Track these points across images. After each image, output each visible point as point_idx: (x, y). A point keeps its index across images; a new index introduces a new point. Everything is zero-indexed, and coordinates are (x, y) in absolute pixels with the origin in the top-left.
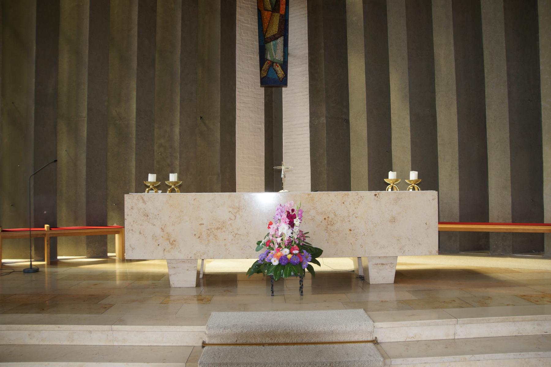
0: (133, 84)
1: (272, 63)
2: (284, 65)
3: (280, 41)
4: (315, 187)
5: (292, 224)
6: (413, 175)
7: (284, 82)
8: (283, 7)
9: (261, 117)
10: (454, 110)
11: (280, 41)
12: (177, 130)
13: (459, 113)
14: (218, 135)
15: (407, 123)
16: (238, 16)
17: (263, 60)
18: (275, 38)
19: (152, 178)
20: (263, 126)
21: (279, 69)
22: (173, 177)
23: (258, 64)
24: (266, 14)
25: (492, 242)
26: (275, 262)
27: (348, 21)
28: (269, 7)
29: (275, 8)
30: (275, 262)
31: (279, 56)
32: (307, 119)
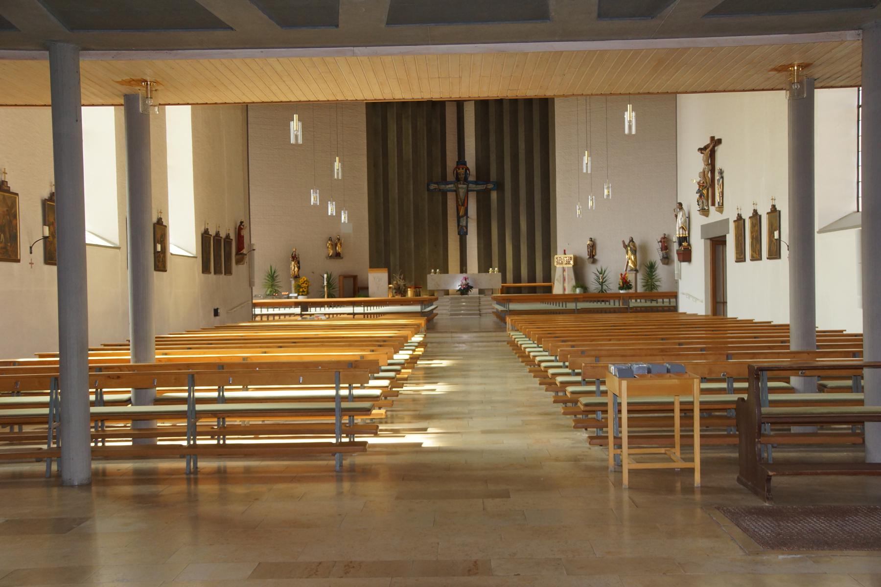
0: (412, 236)
1: (462, 226)
2: (467, 227)
3: (465, 218)
4: (480, 271)
5: (466, 280)
6: (496, 269)
7: (466, 233)
8: (466, 204)
9: (458, 243)
10: (526, 244)
11: (465, 218)
12: (427, 252)
13: (527, 245)
14: (441, 252)
15: (511, 248)
16: (448, 203)
17: (459, 225)
18: (463, 217)
19: (433, 271)
20: (459, 248)
21: (465, 228)
22: (438, 270)
23: (456, 225)
24: (459, 207)
25: (537, 290)
26: (462, 289)
27: (492, 207)
28: (461, 204)
29: (463, 205)
30: (462, 289)
31: (464, 224)
32: (476, 245)
